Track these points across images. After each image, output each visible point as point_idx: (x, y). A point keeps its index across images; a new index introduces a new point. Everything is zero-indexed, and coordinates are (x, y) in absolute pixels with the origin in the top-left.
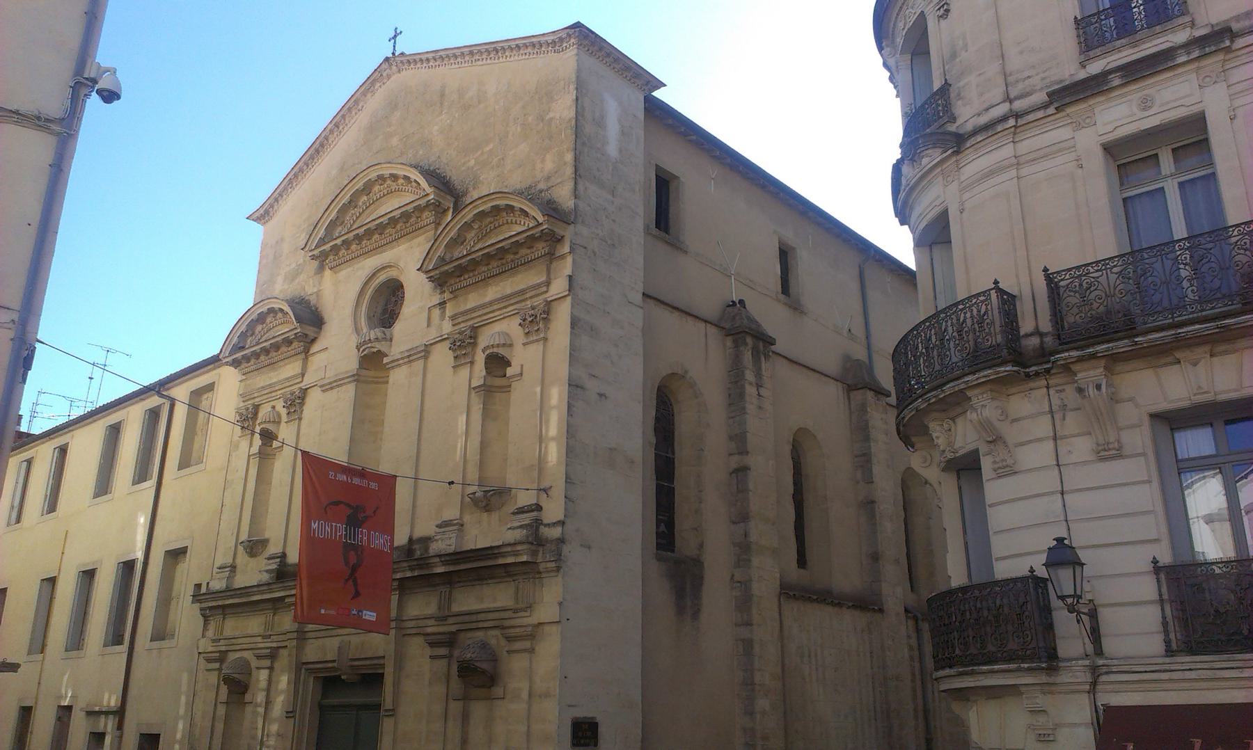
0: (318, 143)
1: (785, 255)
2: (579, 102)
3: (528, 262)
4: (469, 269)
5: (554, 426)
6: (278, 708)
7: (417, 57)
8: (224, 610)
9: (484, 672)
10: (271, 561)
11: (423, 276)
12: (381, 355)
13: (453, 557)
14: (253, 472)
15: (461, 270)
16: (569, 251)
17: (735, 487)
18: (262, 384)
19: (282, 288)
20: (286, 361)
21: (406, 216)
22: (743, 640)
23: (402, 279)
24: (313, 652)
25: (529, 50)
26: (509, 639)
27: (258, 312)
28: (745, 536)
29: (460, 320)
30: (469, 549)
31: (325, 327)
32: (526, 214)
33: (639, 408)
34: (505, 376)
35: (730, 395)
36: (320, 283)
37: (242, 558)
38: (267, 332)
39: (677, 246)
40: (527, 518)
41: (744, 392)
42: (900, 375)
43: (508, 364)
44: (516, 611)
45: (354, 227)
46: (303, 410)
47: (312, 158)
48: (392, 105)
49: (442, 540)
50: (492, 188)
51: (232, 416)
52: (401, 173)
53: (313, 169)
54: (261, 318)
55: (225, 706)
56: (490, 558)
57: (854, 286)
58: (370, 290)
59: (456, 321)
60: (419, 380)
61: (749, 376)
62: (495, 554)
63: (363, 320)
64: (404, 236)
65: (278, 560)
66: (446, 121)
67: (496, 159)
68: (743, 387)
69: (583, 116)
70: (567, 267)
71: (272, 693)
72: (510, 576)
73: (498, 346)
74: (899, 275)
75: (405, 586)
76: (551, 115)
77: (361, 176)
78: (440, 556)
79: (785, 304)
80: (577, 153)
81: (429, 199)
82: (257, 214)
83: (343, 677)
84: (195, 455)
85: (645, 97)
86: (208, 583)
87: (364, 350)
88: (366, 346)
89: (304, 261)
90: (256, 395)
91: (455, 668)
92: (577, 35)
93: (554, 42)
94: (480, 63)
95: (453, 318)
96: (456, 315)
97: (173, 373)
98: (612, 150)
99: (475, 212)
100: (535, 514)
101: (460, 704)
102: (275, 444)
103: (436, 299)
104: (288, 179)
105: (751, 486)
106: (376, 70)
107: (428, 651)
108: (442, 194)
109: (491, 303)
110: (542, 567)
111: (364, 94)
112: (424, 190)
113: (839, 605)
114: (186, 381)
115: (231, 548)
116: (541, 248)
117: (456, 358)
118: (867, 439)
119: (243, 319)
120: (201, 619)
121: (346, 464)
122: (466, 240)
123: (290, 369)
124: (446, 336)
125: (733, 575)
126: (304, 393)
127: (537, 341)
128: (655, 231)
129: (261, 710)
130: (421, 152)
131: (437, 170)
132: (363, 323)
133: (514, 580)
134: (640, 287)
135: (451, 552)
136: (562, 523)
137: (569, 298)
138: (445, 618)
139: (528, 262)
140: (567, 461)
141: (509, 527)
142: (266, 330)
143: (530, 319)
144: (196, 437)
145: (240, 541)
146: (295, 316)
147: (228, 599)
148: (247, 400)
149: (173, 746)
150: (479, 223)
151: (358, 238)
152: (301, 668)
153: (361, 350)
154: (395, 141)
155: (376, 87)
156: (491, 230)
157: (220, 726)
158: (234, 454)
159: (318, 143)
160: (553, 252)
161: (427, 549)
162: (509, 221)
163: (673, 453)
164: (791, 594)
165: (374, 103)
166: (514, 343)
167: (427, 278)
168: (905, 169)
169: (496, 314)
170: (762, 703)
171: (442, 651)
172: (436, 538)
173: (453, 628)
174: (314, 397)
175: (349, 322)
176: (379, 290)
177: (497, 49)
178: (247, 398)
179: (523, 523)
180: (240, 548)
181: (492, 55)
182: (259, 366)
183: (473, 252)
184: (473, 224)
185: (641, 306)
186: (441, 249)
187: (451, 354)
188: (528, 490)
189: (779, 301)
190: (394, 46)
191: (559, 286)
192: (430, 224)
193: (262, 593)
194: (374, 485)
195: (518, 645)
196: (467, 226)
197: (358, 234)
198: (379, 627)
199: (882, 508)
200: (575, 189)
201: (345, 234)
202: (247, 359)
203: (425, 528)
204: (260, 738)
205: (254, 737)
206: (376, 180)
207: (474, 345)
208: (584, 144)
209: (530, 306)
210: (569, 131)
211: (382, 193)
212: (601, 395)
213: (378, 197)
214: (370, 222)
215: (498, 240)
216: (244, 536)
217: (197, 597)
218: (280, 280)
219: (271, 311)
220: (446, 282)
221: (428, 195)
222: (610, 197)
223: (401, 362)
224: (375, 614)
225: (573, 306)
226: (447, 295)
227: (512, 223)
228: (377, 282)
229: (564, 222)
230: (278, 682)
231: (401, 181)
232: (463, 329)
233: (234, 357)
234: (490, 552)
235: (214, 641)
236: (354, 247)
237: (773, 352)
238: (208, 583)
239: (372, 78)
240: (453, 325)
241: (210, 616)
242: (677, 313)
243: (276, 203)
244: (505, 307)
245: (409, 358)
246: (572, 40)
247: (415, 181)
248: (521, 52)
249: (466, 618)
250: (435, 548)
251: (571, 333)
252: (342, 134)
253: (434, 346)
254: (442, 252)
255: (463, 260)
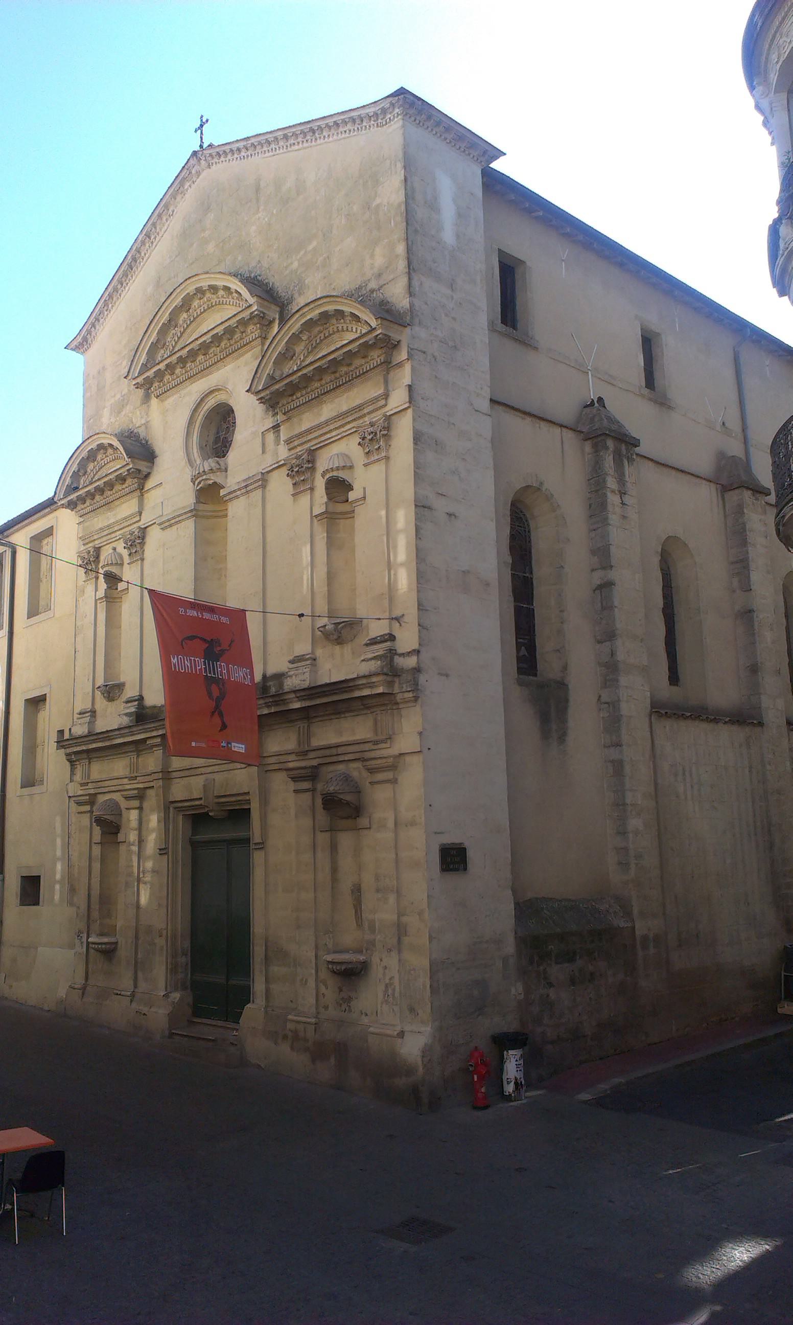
0: (129, 257)
1: (649, 343)
2: (409, 183)
3: (364, 373)
4: (300, 386)
5: (403, 551)
6: (152, 842)
7: (227, 148)
8: (90, 755)
9: (348, 803)
10: (130, 705)
11: (253, 399)
12: (217, 486)
13: (307, 693)
14: (102, 616)
15: (293, 389)
16: (406, 357)
17: (600, 604)
18: (100, 526)
19: (110, 422)
20: (122, 500)
21: (230, 332)
22: (612, 761)
23: (232, 403)
24: (178, 791)
25: (349, 126)
26: (371, 771)
27: (88, 450)
28: (612, 655)
29: (296, 443)
30: (324, 683)
31: (157, 461)
32: (356, 318)
33: (493, 525)
34: (348, 501)
35: (590, 506)
36: (147, 414)
37: (101, 703)
38: (99, 469)
39: (527, 343)
40: (380, 649)
41: (606, 501)
42: (779, 469)
43: (350, 487)
44: (376, 743)
45: (176, 349)
46: (144, 550)
47: (125, 275)
48: (205, 206)
49: (296, 675)
50: (319, 292)
51: (75, 560)
52: (220, 283)
53: (127, 288)
54: (92, 456)
55: (99, 846)
56: (346, 692)
57: (728, 373)
58: (200, 418)
59: (292, 445)
60: (259, 510)
61: (611, 483)
62: (349, 687)
63: (195, 450)
64: (230, 354)
65: (136, 703)
66: (264, 219)
67: (321, 258)
68: (605, 495)
69: (413, 198)
70: (405, 376)
71: (144, 833)
72: (368, 708)
73: (338, 469)
74: (779, 356)
75: (264, 723)
76: (378, 201)
77: (178, 290)
78: (295, 692)
79: (650, 399)
80: (410, 243)
81: (252, 311)
82: (75, 343)
83: (210, 814)
84: (42, 603)
85: (482, 169)
86: (70, 729)
87: (199, 483)
88: (201, 479)
89: (129, 390)
90: (95, 537)
91: (319, 801)
92: (401, 103)
93: (376, 115)
94: (296, 147)
95: (288, 441)
96: (290, 438)
97: (10, 519)
98: (448, 236)
99: (303, 321)
100: (388, 644)
101: (328, 835)
102: (121, 586)
103: (269, 422)
104: (103, 300)
105: (616, 603)
106: (184, 167)
107: (292, 786)
108: (266, 303)
109: (327, 423)
110: (399, 697)
111: (174, 196)
112: (246, 300)
113: (716, 721)
114: (26, 525)
115: (88, 693)
116: (376, 356)
117: (294, 484)
118: (744, 543)
119: (74, 457)
120: (68, 763)
121: (193, 601)
122: (295, 354)
123: (127, 508)
124: (283, 462)
125: (600, 696)
126: (144, 533)
127: (378, 460)
128: (500, 327)
129: (135, 848)
130: (240, 258)
131: (258, 277)
132: (196, 455)
133: (371, 713)
134: (487, 393)
135: (306, 686)
136: (417, 652)
137: (410, 411)
138: (305, 753)
139: (364, 373)
140: (417, 587)
141: (362, 659)
142: (97, 468)
143: (370, 437)
144: (41, 584)
145: (96, 687)
146: (125, 452)
147: (91, 743)
148: (87, 544)
149: (54, 887)
150: (307, 333)
151: (182, 361)
152: (169, 807)
153: (196, 484)
154: (211, 248)
155: (186, 187)
156: (321, 341)
157: (97, 866)
158: (80, 600)
159: (129, 257)
160: (389, 360)
161: (281, 685)
162: (340, 328)
163: (531, 573)
164: (663, 712)
165: (185, 206)
166: (355, 465)
167: (258, 400)
168: (783, 230)
169: (334, 434)
170: (634, 823)
171: (306, 785)
172: (290, 673)
173: (315, 763)
174: (154, 537)
175: (181, 453)
176: (209, 417)
177: (313, 130)
178: (87, 541)
179: (377, 654)
180: (98, 694)
181: (308, 137)
182: (95, 506)
183: (304, 367)
184: (301, 335)
185: (489, 413)
186: (269, 367)
187: (289, 482)
188: (380, 619)
189: (643, 396)
190: (201, 138)
191: (398, 398)
192: (256, 338)
193: (122, 736)
194: (224, 620)
195: (380, 776)
196: (295, 338)
197: (181, 356)
198: (246, 760)
199: (761, 617)
200: (410, 285)
201: (169, 357)
202: (82, 500)
203: (277, 665)
204: (136, 875)
205: (130, 874)
206: (195, 294)
207: (313, 469)
208: (416, 231)
209: (368, 423)
210: (399, 219)
211: (202, 308)
212: (450, 515)
213: (199, 313)
214: (193, 341)
215: (329, 351)
216: (100, 681)
217: (61, 742)
218: (106, 413)
219: (101, 447)
220: (278, 403)
221: (251, 305)
222: (449, 292)
223: (239, 493)
224: (243, 746)
225: (414, 420)
226: (280, 417)
227: (343, 330)
228: (206, 408)
229: (400, 325)
230: (148, 821)
231: (221, 293)
232: (299, 454)
233: (69, 498)
234: (345, 685)
235: (82, 785)
236: (178, 371)
237: (637, 455)
238: (70, 729)
239: (180, 177)
240: (290, 450)
241: (75, 761)
242: (529, 419)
243: (93, 329)
244: (342, 426)
245: (246, 488)
246: (397, 110)
247: (237, 292)
248: (341, 129)
249: (327, 752)
250: (291, 683)
251: (415, 450)
252: (154, 244)
253: (271, 474)
254: (270, 369)
255: (294, 377)
